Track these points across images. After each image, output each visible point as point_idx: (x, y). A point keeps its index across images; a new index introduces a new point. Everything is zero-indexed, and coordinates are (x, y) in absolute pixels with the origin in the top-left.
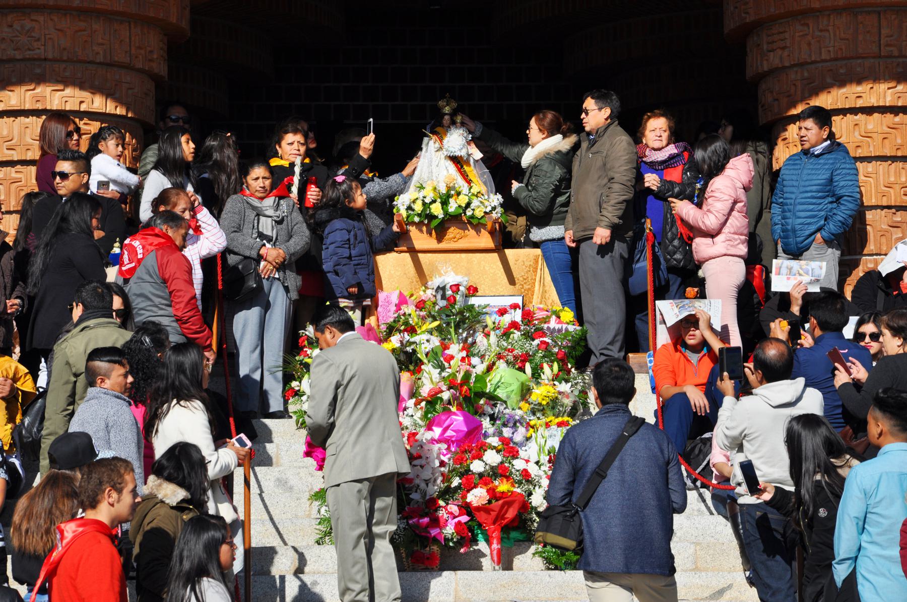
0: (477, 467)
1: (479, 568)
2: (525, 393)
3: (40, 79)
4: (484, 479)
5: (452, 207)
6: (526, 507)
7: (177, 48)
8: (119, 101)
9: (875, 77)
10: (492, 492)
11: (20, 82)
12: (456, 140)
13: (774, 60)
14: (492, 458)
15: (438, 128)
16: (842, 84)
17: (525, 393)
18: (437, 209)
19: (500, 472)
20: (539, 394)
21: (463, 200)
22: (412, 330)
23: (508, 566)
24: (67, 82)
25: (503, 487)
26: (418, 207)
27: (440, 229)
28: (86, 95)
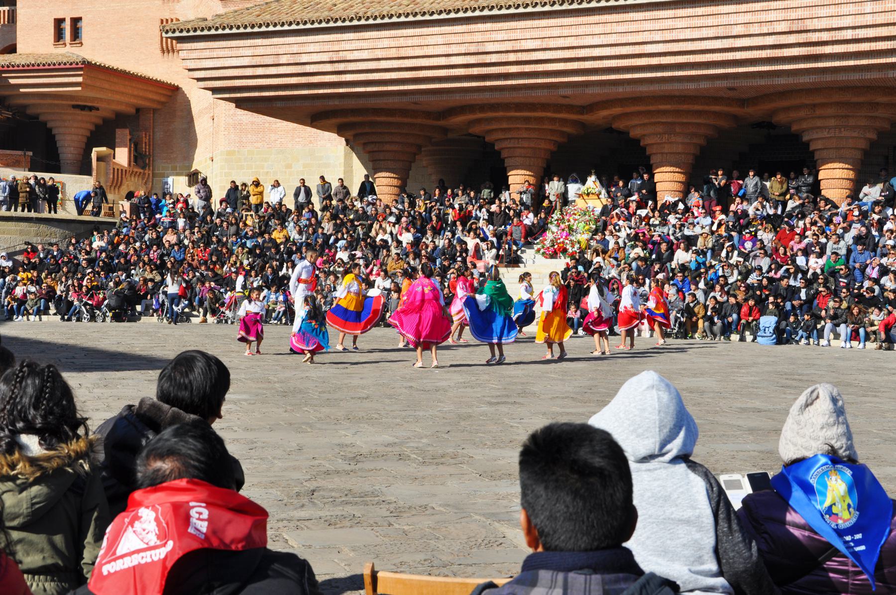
3: (518, 169)
15: (590, 174)
19: (563, 243)
20: (587, 227)
27: (588, 194)
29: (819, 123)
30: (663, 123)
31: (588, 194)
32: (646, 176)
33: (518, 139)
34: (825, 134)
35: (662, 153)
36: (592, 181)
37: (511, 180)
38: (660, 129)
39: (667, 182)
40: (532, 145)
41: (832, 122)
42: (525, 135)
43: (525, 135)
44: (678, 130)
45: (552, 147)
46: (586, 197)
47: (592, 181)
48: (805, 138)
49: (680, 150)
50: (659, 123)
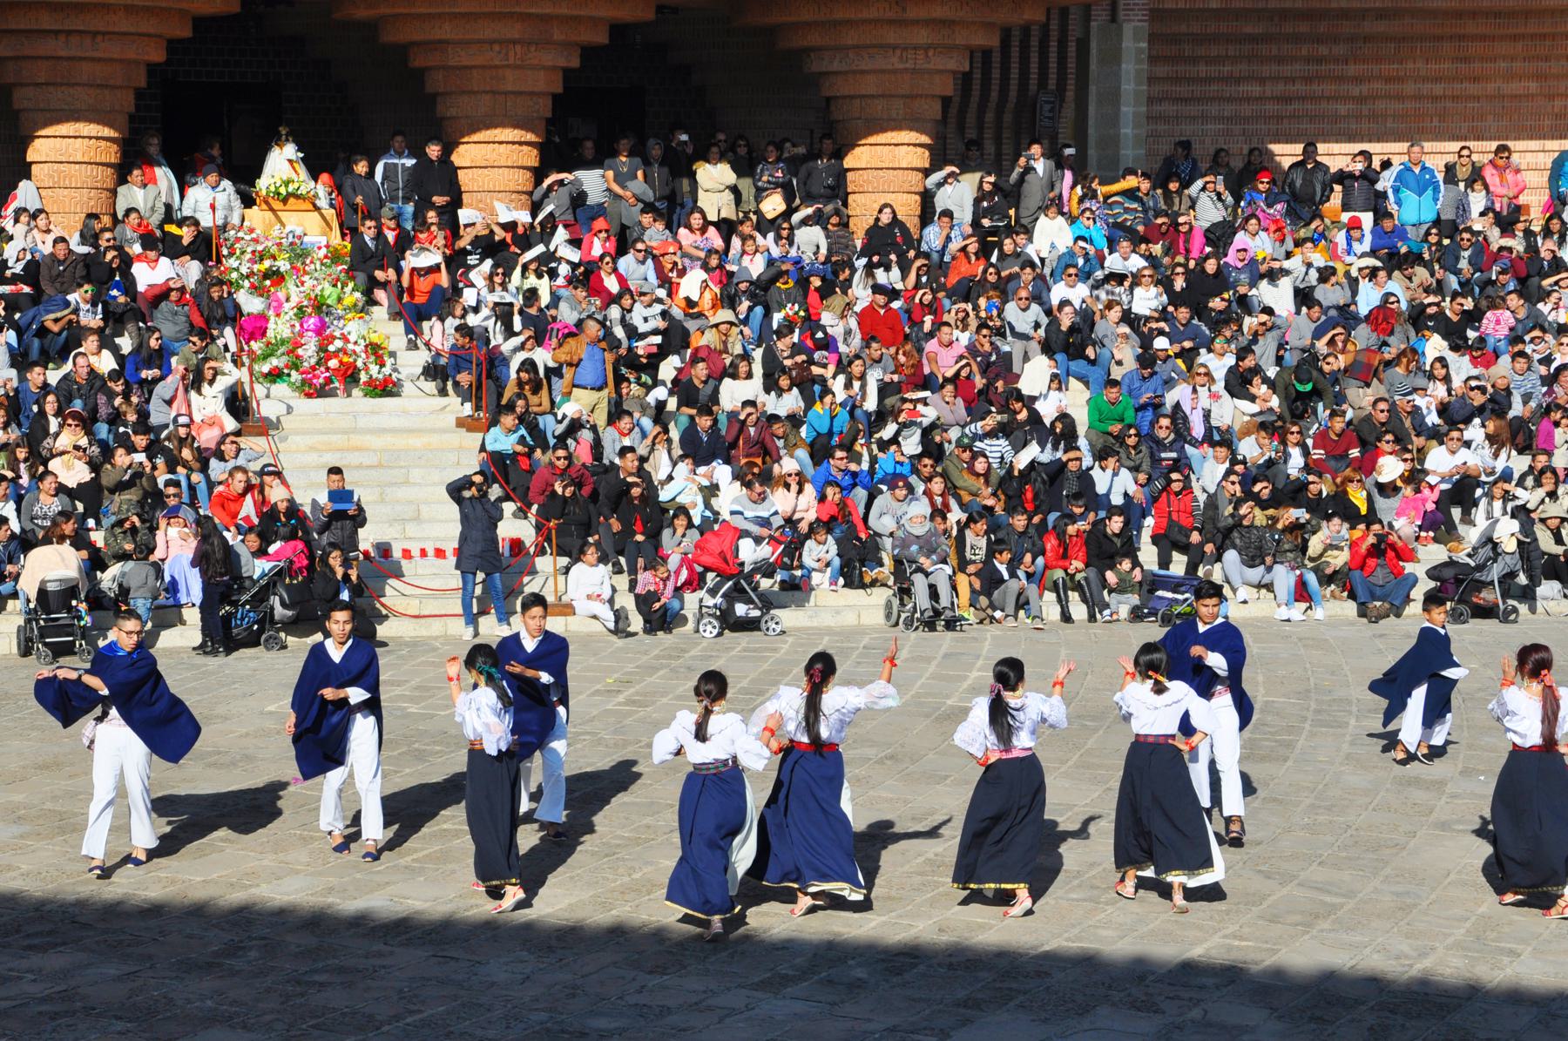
0: (331, 348)
1: (336, 395)
2: (340, 300)
3: (77, 120)
4: (335, 354)
5: (290, 189)
6: (353, 366)
7: (139, 94)
8: (116, 130)
9: (503, 125)
10: (341, 362)
11: (67, 121)
12: (290, 150)
13: (453, 112)
14: (338, 344)
16: (488, 128)
17: (340, 300)
18: (283, 191)
21: (296, 185)
22: (274, 258)
23: (349, 395)
24: (90, 121)
25: (346, 359)
26: (272, 189)
28: (100, 127)
29: (892, 36)
30: (524, 17)
31: (285, 201)
32: (433, 151)
33: (95, 34)
34: (894, 62)
35: (494, 93)
36: (282, 165)
37: (39, 150)
38: (514, 31)
39: (493, 171)
40: (131, 54)
41: (922, 36)
42: (124, 25)
43: (124, 25)
44: (558, 35)
45: (158, 55)
46: (277, 205)
47: (282, 165)
48: (816, 65)
49: (541, 86)
50: (511, 15)
